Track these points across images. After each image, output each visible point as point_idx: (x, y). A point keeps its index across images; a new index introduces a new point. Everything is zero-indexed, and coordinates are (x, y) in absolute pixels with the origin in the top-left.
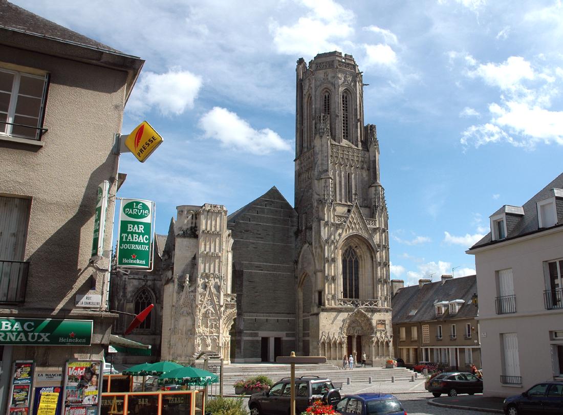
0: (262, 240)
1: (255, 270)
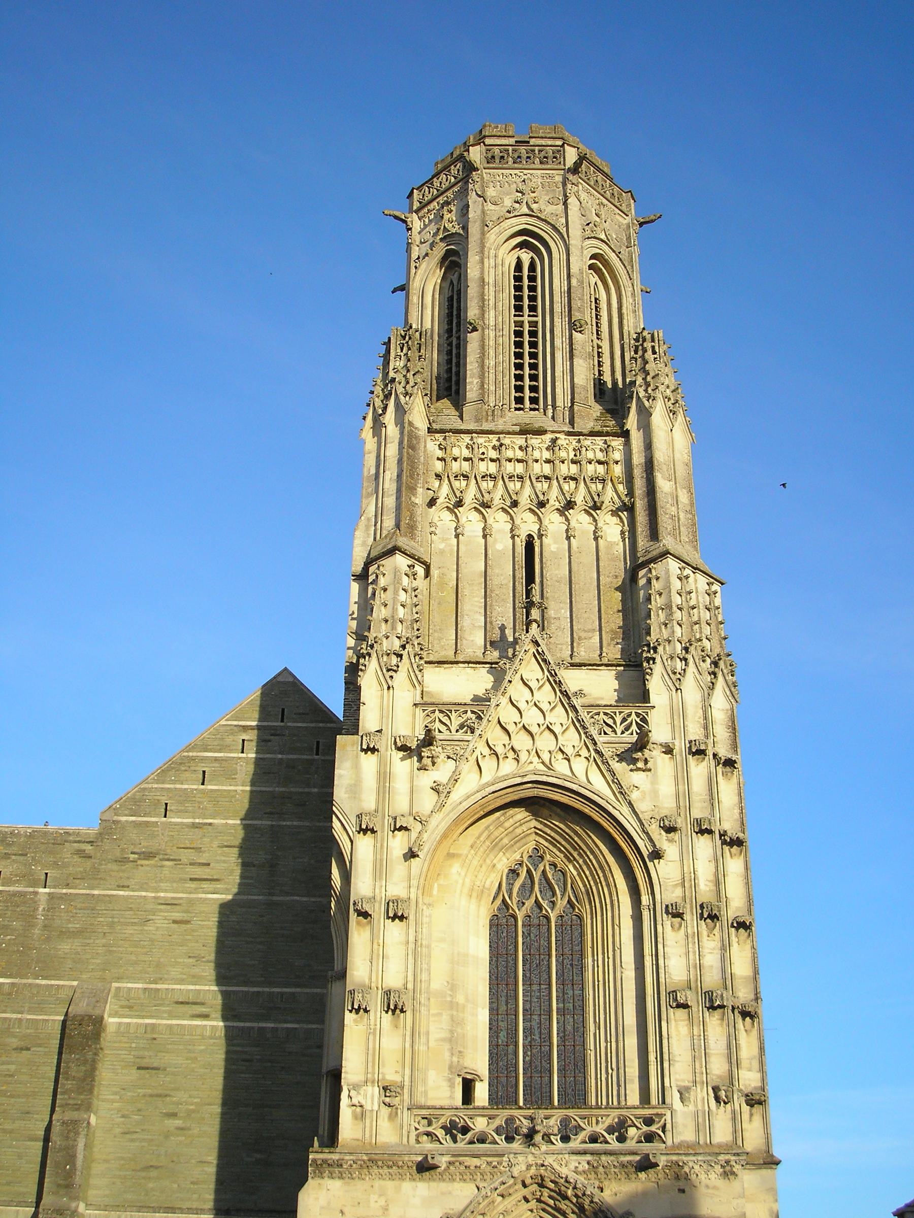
0: (219, 886)
1: (171, 1016)
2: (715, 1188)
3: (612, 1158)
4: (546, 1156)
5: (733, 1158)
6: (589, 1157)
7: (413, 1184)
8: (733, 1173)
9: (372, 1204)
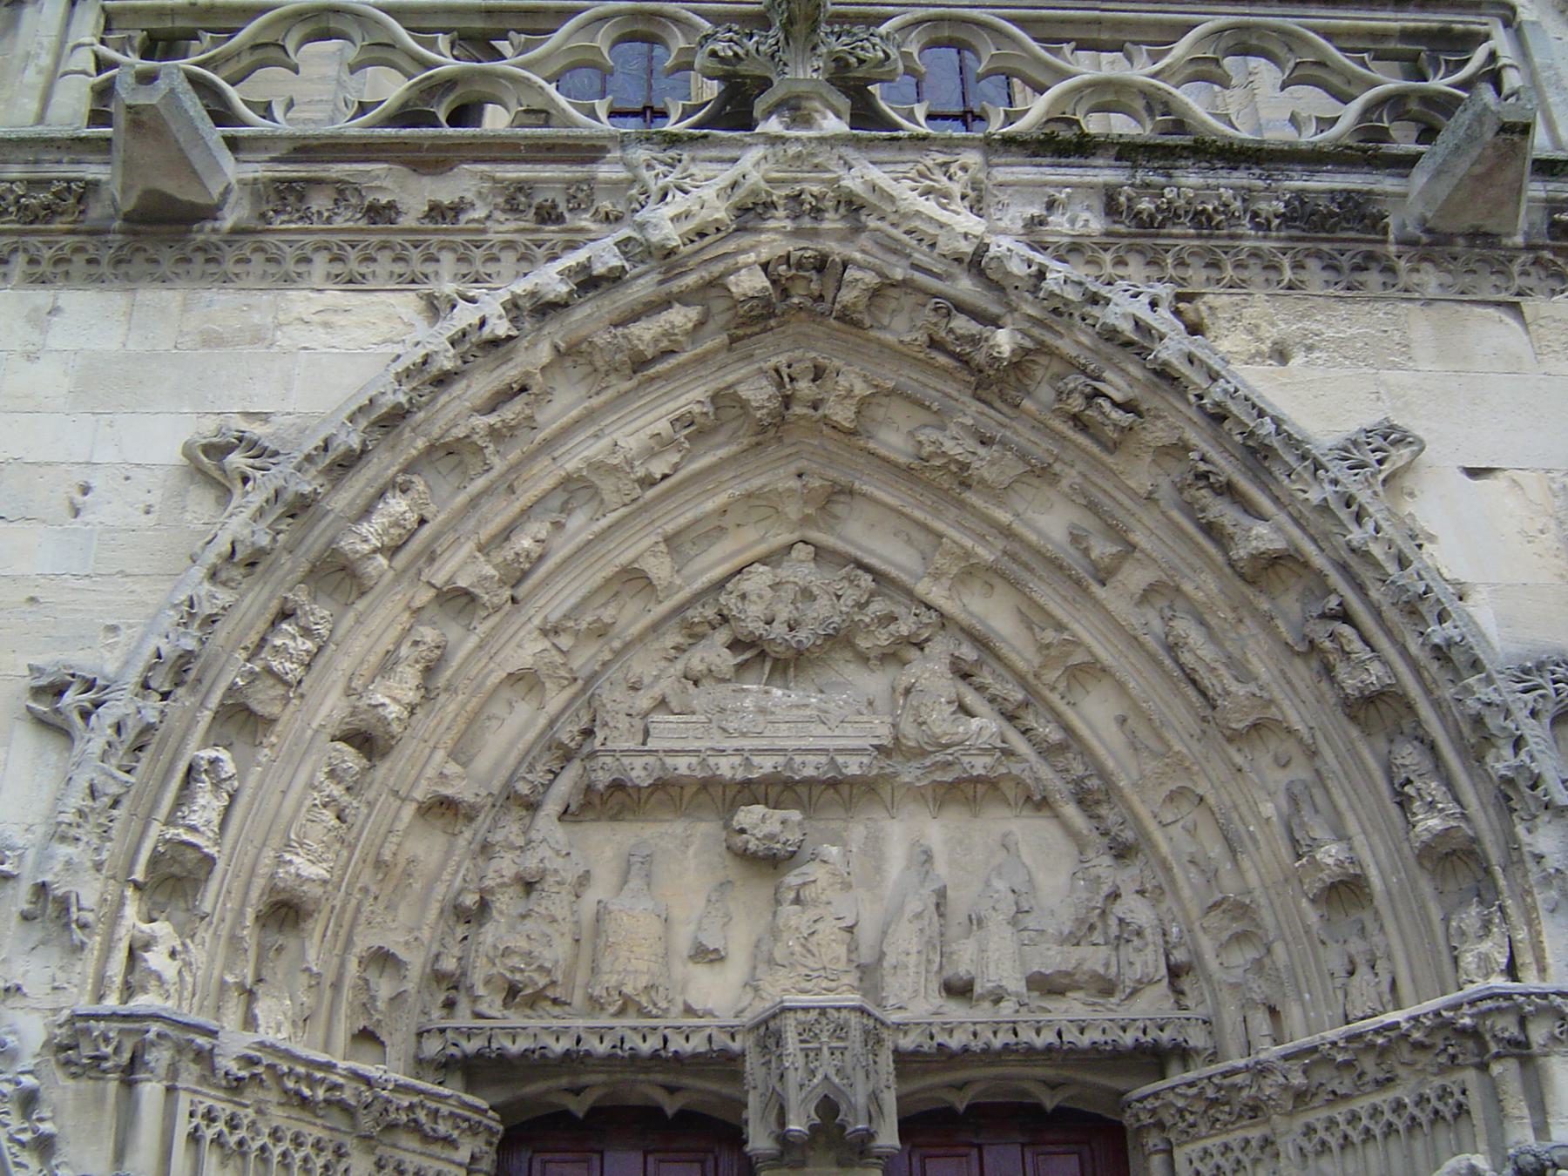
3: (1240, 178)
4: (850, 154)
6: (1105, 174)
7: (41, 297)
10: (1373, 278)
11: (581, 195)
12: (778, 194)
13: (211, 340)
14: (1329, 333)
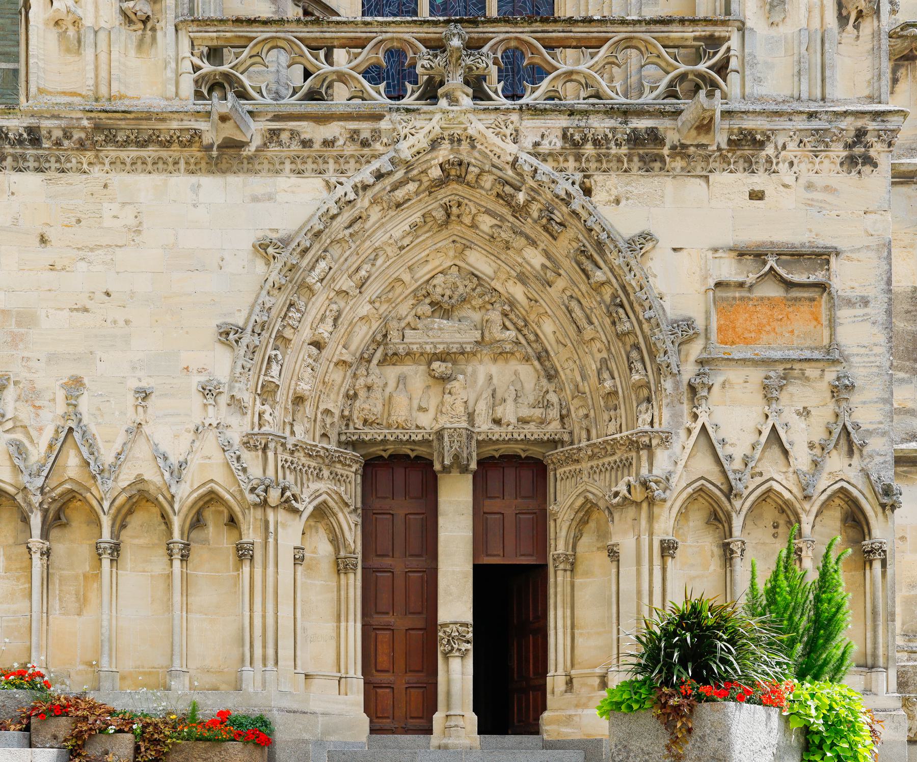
2: (827, 189)
5: (872, 126)
7: (193, 179)
8: (869, 161)
9: (108, 222)
10: (657, 165)
11: (376, 134)
12: (446, 134)
13: (255, 199)
14: (636, 192)
